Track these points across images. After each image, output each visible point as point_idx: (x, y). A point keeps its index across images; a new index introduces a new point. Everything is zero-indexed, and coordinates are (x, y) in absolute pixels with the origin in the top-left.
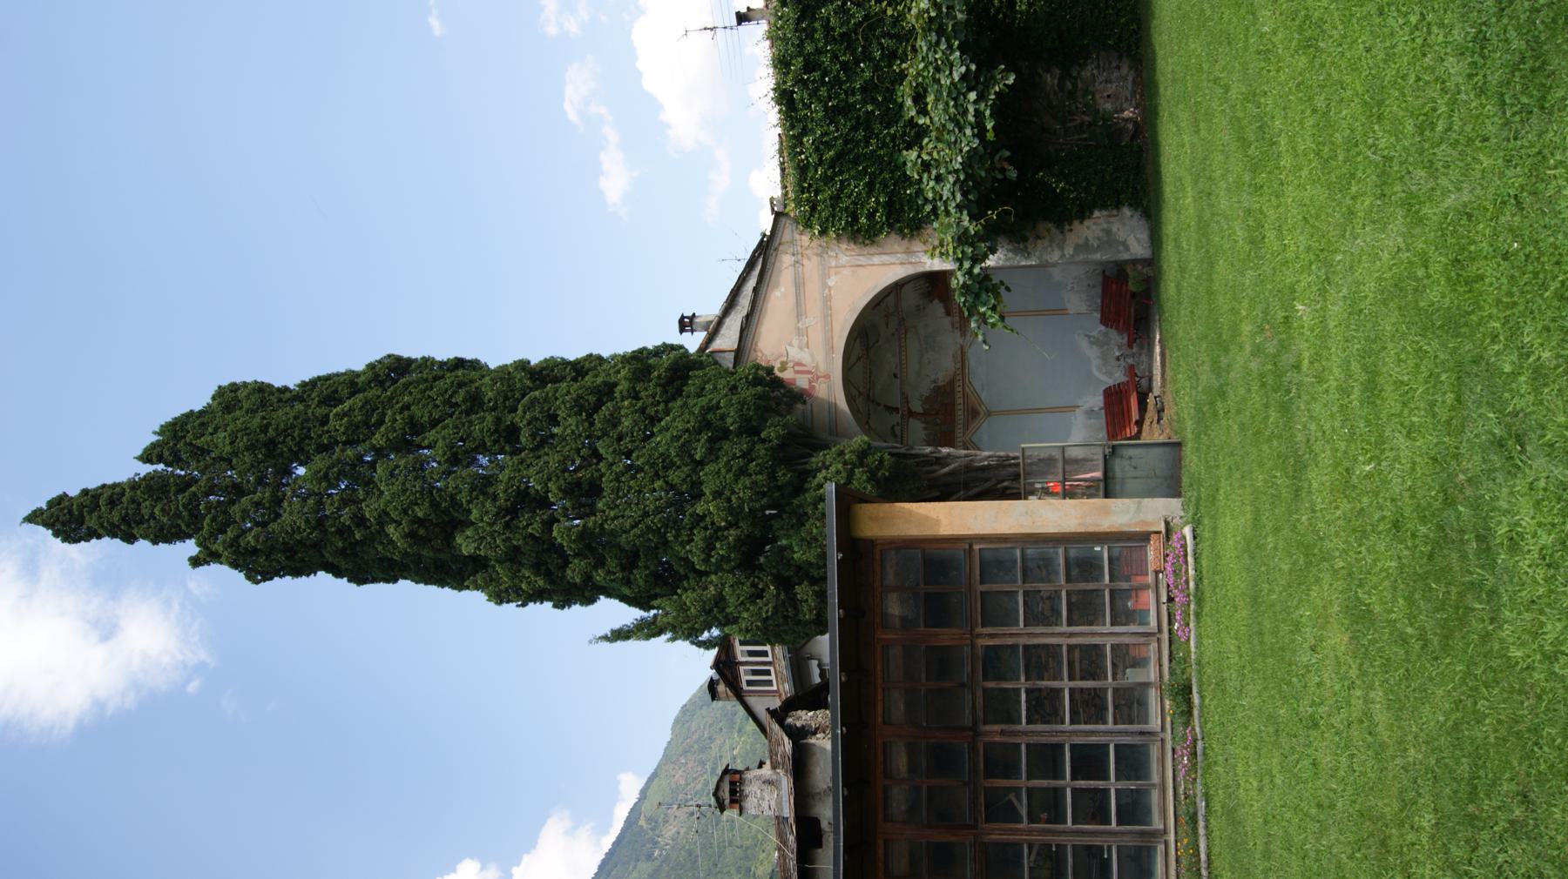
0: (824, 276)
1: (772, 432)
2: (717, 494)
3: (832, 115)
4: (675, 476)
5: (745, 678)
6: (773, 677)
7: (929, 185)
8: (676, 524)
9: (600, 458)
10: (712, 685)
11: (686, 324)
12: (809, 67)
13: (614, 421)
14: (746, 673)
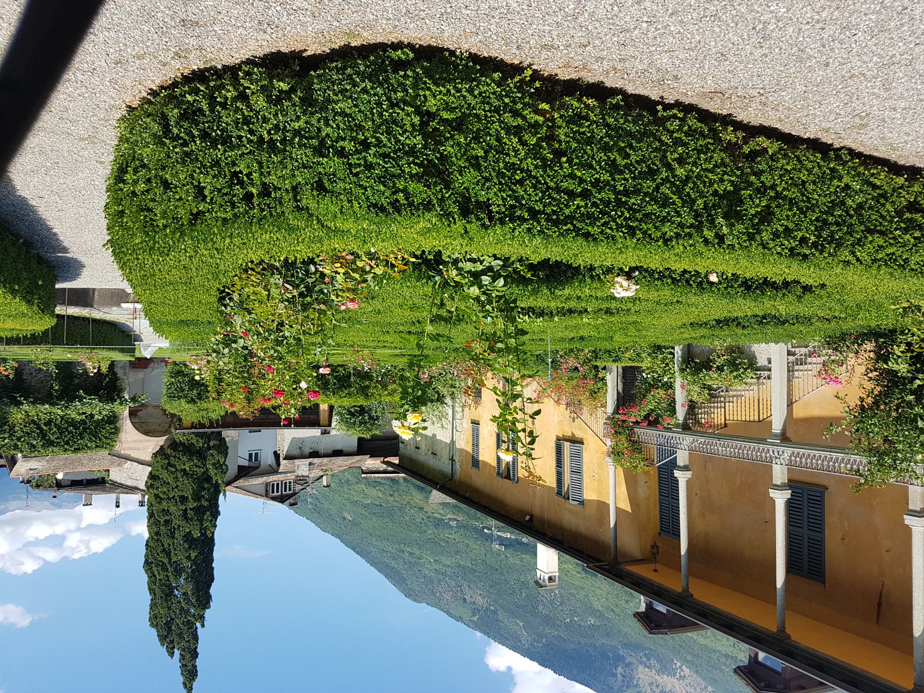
0: (128, 442)
1: (169, 451)
2: (184, 464)
3: (82, 438)
4: (179, 476)
5: (288, 492)
6: (288, 481)
7: (104, 413)
8: (193, 475)
9: (174, 496)
10: (292, 505)
11: (142, 504)
12: (67, 443)
13: (164, 493)
14: (285, 491)
